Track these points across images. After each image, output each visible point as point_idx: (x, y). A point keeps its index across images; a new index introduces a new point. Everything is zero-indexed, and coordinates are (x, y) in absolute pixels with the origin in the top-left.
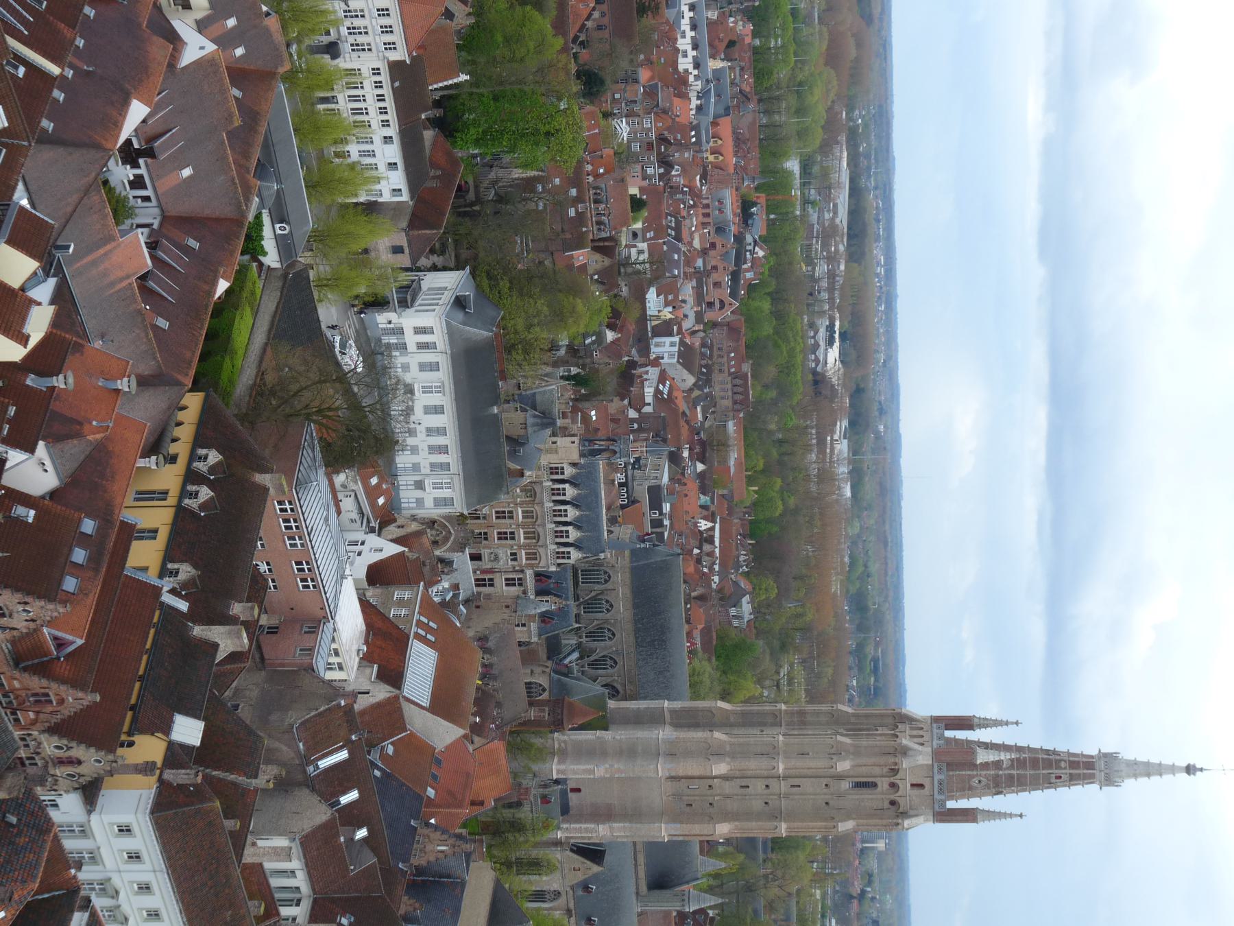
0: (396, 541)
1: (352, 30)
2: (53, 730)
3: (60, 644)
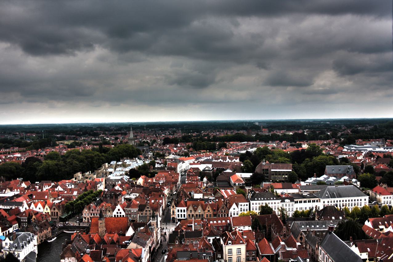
1: (387, 203)
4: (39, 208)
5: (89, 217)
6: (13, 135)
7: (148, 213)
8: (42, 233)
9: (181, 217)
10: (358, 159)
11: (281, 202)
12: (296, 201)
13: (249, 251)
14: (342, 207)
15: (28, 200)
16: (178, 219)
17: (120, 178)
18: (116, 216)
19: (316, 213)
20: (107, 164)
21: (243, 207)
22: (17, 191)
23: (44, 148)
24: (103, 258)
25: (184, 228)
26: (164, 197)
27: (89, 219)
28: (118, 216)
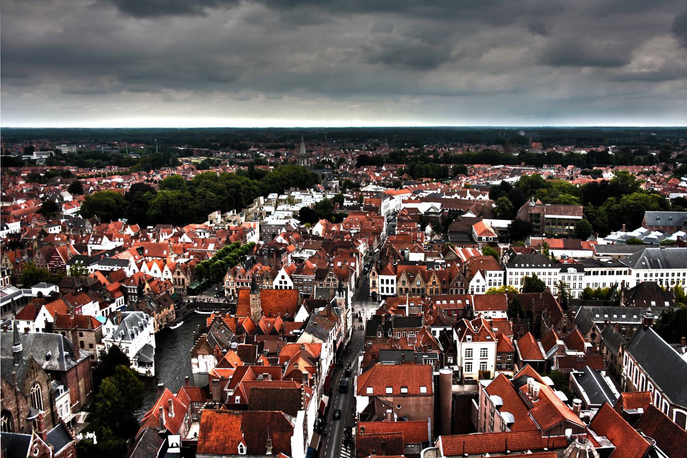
4: (154, 271)
5: (234, 289)
6: (110, 145)
7: (332, 283)
8: (160, 313)
9: (388, 291)
11: (561, 272)
12: (586, 272)
13: (502, 352)
14: (670, 285)
15: (136, 256)
16: (382, 296)
17: (284, 224)
18: (279, 288)
19: (623, 294)
20: (262, 198)
21: (493, 278)
22: (119, 241)
23: (159, 168)
24: (258, 358)
25: (392, 310)
26: (358, 258)
27: (235, 291)
28: (281, 287)
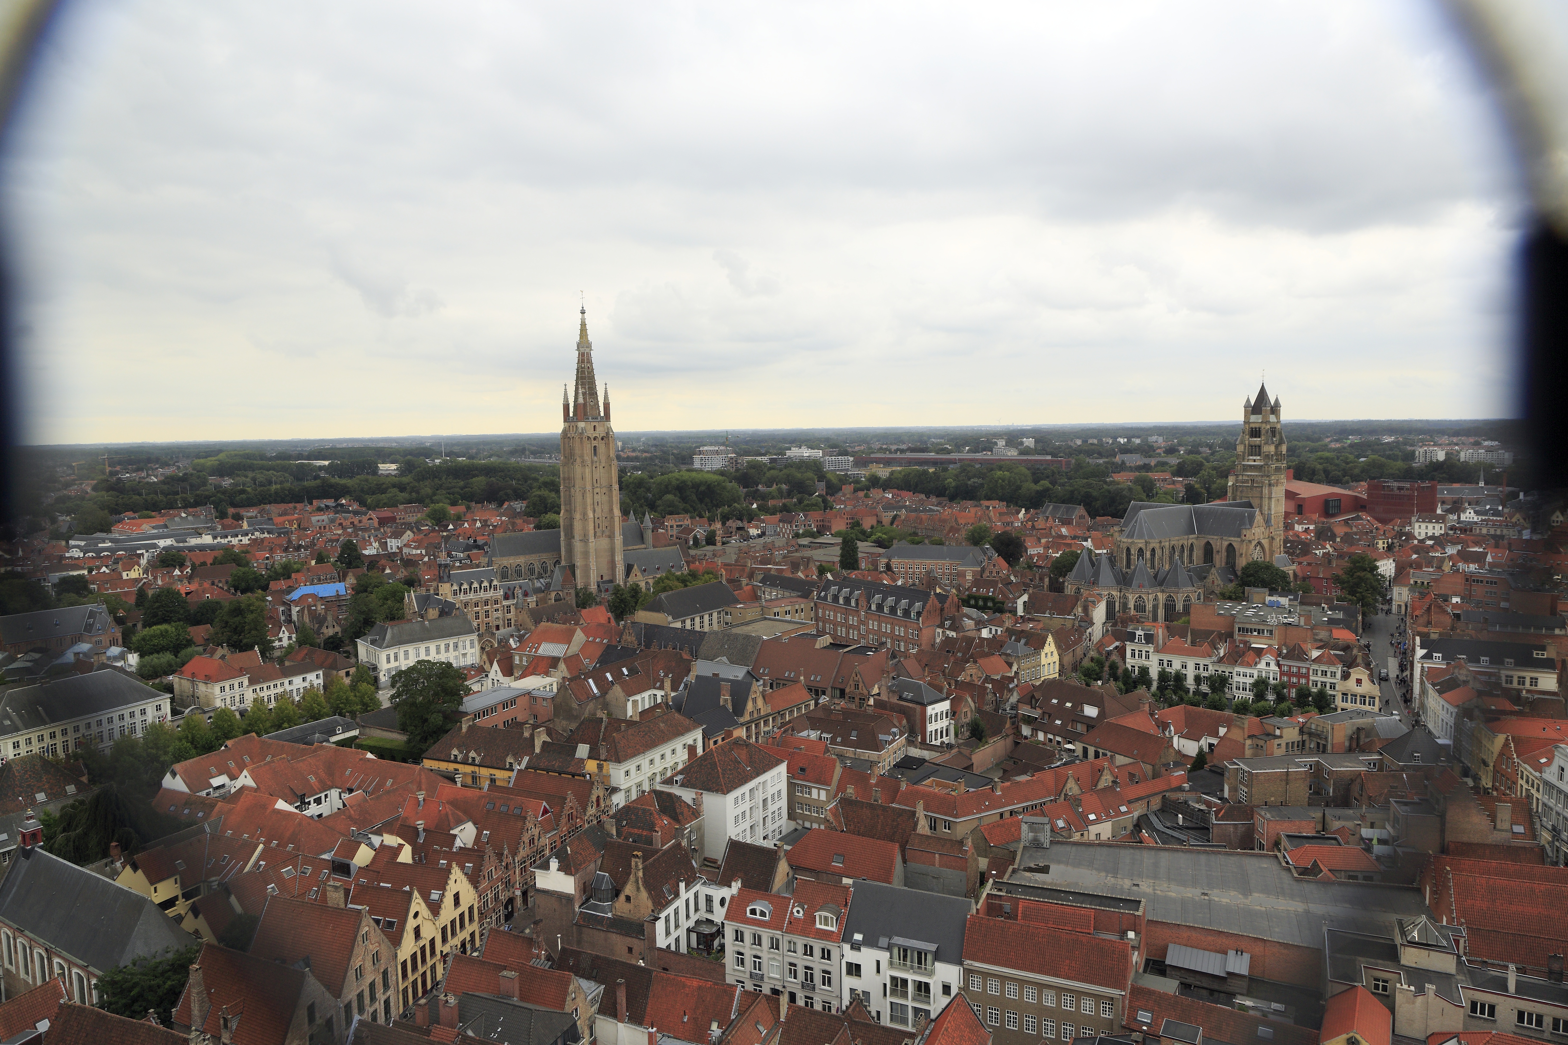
0: (491, 665)
2: (585, 810)
3: (546, 811)
10: (125, 577)
